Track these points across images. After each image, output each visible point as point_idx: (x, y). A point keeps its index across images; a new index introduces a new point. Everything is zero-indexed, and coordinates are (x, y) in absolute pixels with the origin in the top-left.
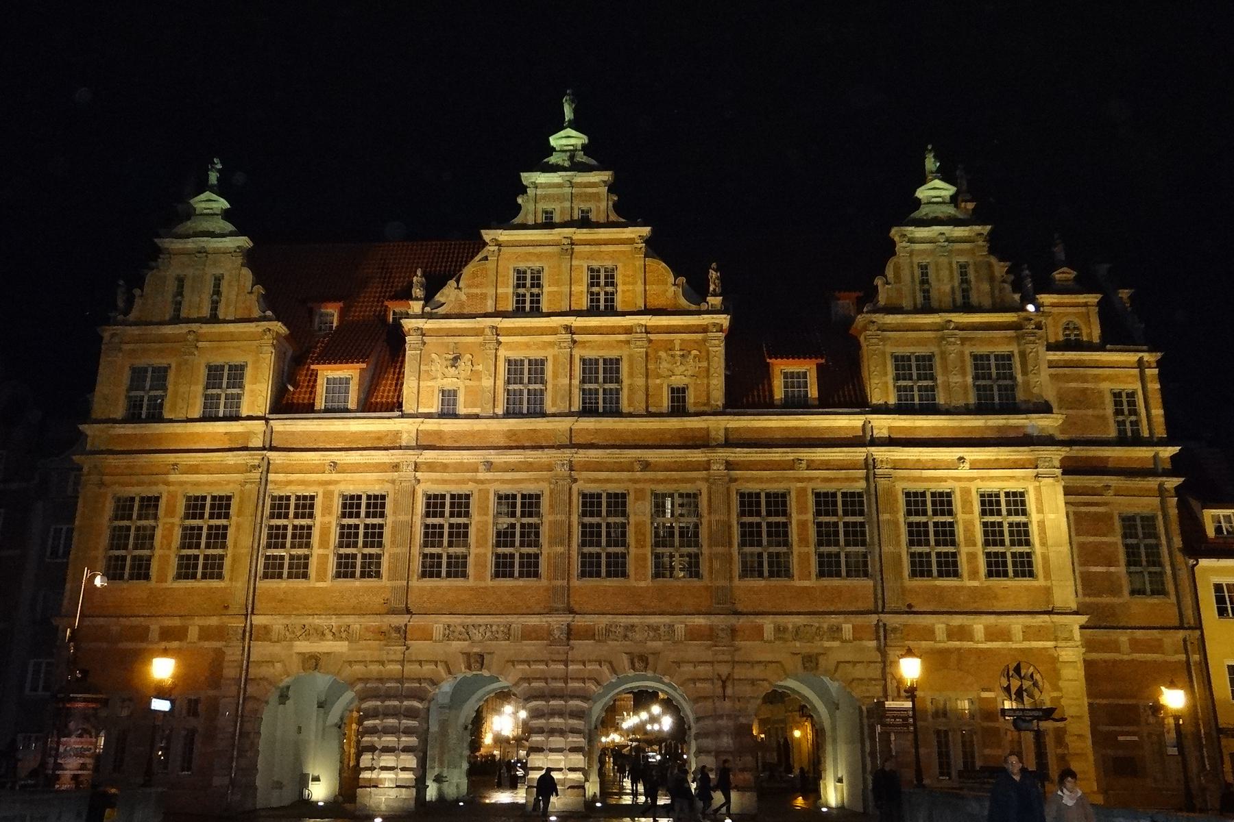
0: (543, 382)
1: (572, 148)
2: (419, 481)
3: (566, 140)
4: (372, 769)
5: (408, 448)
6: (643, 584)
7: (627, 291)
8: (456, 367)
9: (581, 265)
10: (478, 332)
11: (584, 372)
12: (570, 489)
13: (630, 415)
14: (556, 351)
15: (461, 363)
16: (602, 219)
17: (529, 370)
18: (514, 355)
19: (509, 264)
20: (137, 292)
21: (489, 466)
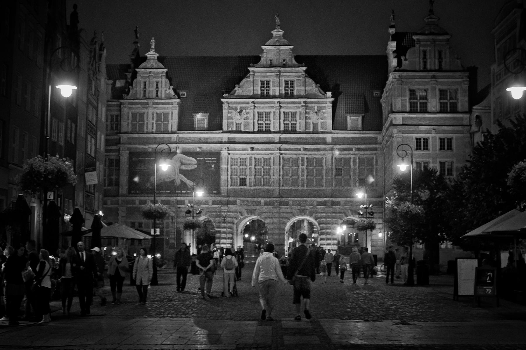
0: (270, 121)
1: (279, 35)
2: (229, 154)
3: (277, 33)
4: (219, 243)
5: (225, 143)
6: (303, 188)
7: (298, 89)
8: (240, 115)
9: (283, 79)
10: (248, 103)
11: (285, 117)
12: (280, 158)
13: (300, 133)
14: (274, 110)
15: (242, 114)
16: (290, 63)
17: (266, 116)
18: (261, 111)
19: (259, 79)
20: (130, 87)
21: (252, 149)
